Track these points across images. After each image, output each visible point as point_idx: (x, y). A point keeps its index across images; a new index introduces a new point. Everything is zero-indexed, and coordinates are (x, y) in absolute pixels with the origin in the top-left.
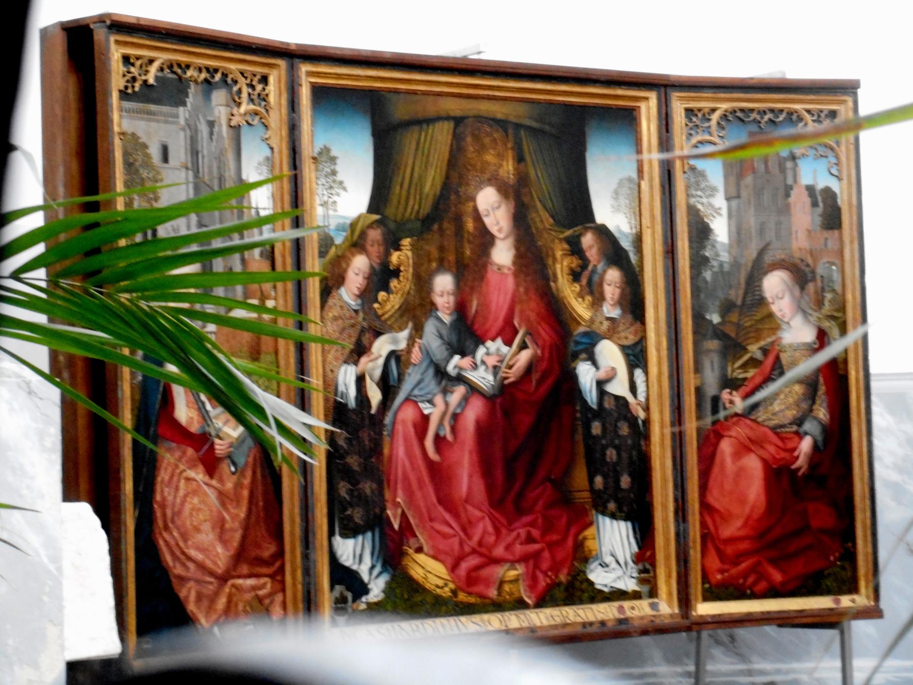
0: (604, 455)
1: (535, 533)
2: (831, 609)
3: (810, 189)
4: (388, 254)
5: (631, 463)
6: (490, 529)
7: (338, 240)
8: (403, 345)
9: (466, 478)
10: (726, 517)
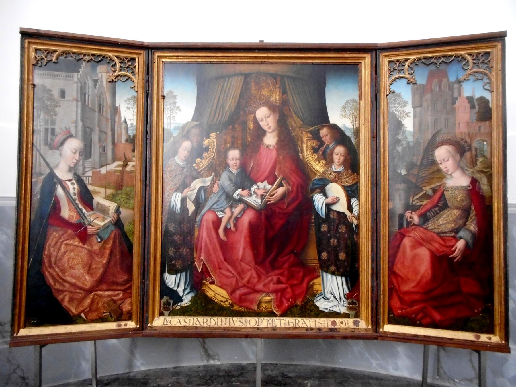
0: (329, 241)
1: (283, 279)
2: (473, 341)
3: (470, 99)
4: (203, 140)
5: (347, 246)
6: (255, 275)
7: (175, 134)
8: (208, 184)
9: (241, 248)
10: (406, 280)
